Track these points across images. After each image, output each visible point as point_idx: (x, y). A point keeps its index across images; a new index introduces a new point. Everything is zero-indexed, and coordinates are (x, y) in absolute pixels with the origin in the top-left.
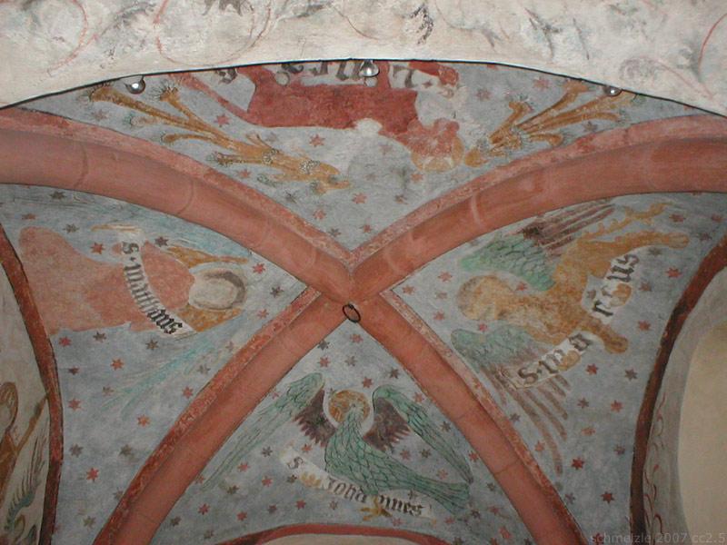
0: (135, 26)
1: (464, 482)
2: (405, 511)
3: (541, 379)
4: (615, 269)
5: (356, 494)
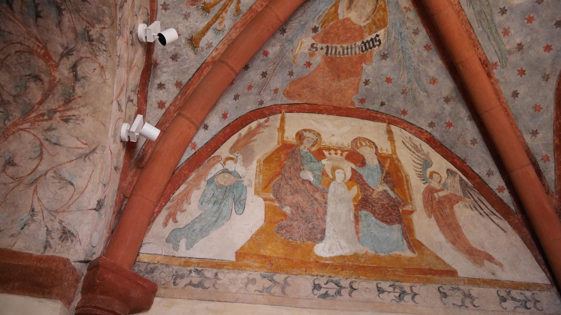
0: (94, 37)
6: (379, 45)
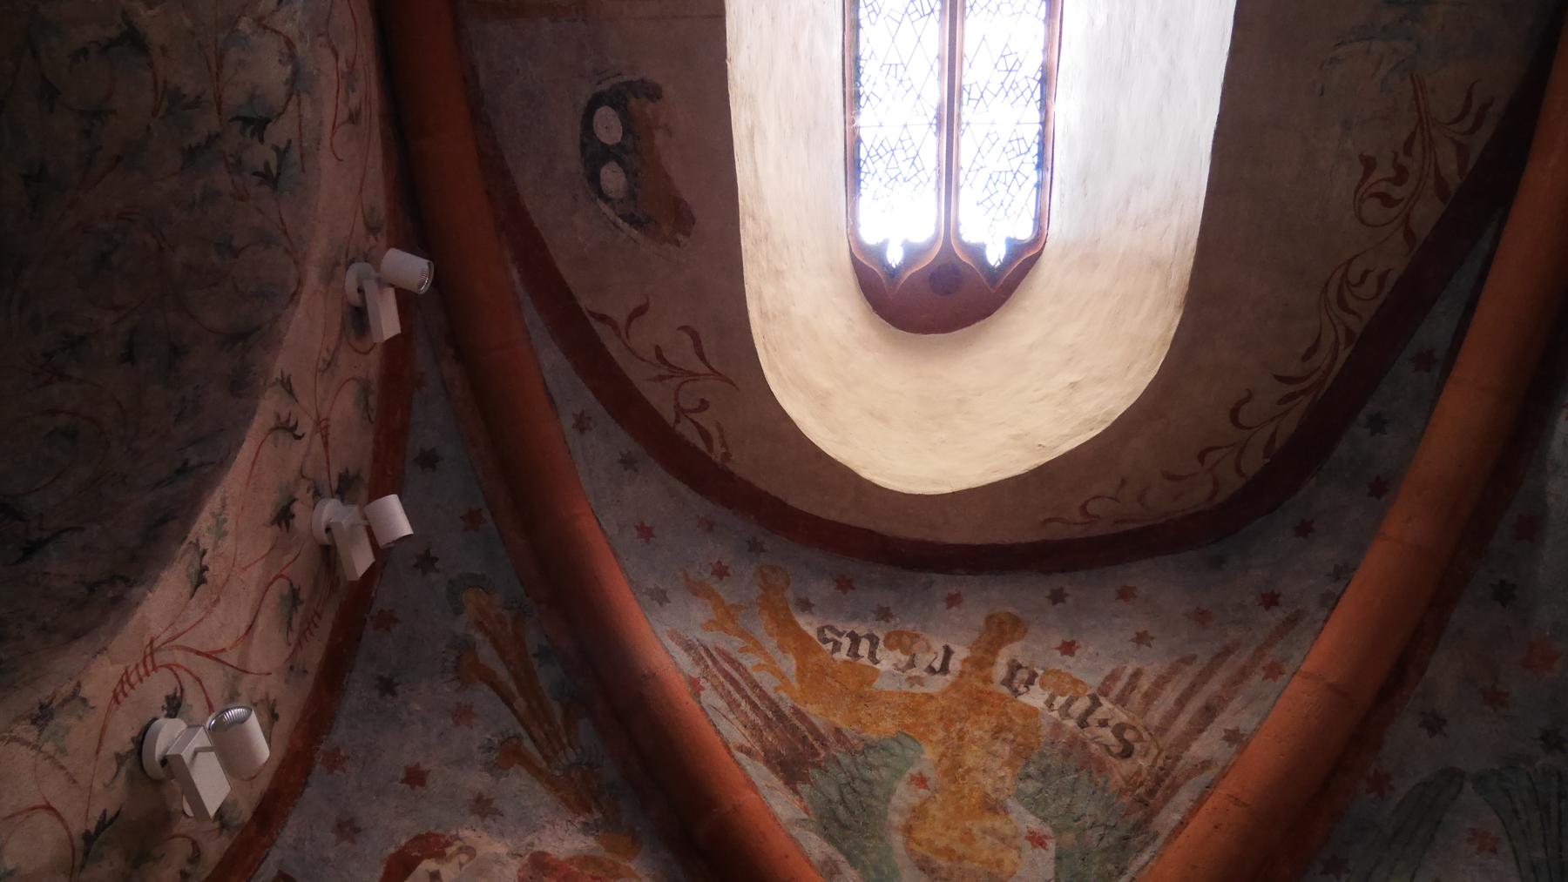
1: (1468, 786)
3: (1121, 716)
4: (856, 656)
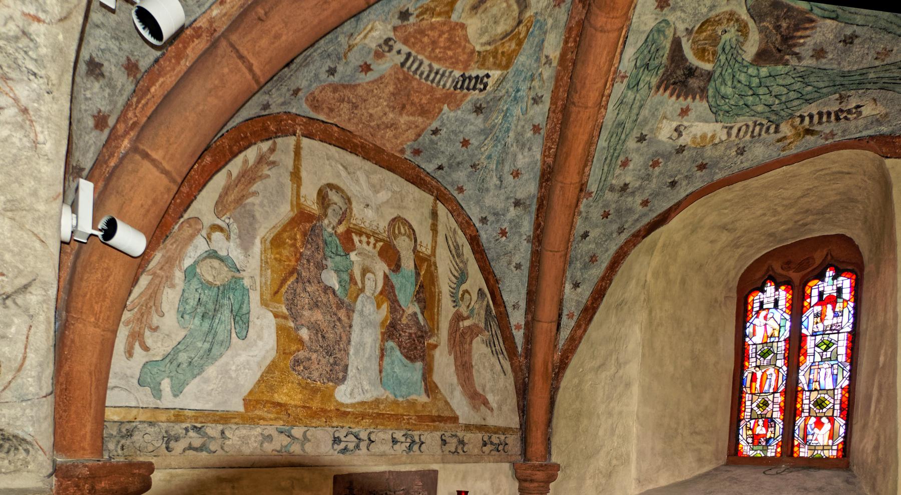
2: (838, 119)
5: (765, 127)
6: (481, 90)
